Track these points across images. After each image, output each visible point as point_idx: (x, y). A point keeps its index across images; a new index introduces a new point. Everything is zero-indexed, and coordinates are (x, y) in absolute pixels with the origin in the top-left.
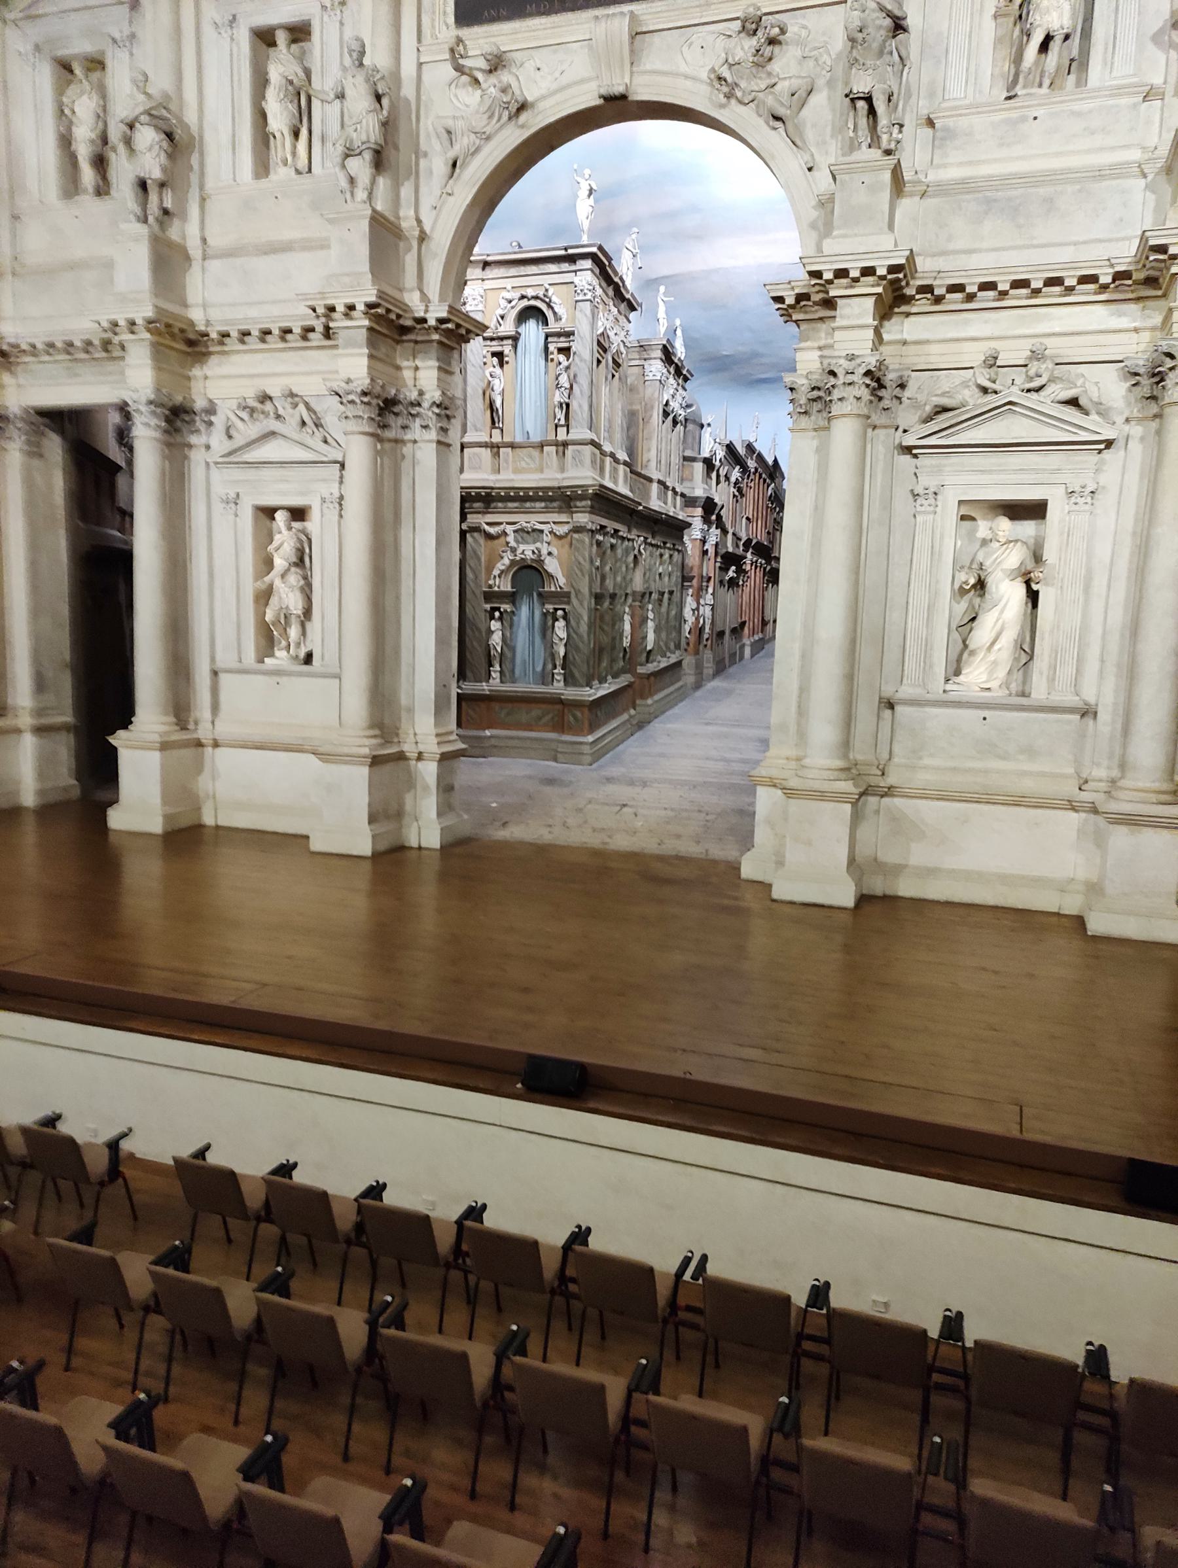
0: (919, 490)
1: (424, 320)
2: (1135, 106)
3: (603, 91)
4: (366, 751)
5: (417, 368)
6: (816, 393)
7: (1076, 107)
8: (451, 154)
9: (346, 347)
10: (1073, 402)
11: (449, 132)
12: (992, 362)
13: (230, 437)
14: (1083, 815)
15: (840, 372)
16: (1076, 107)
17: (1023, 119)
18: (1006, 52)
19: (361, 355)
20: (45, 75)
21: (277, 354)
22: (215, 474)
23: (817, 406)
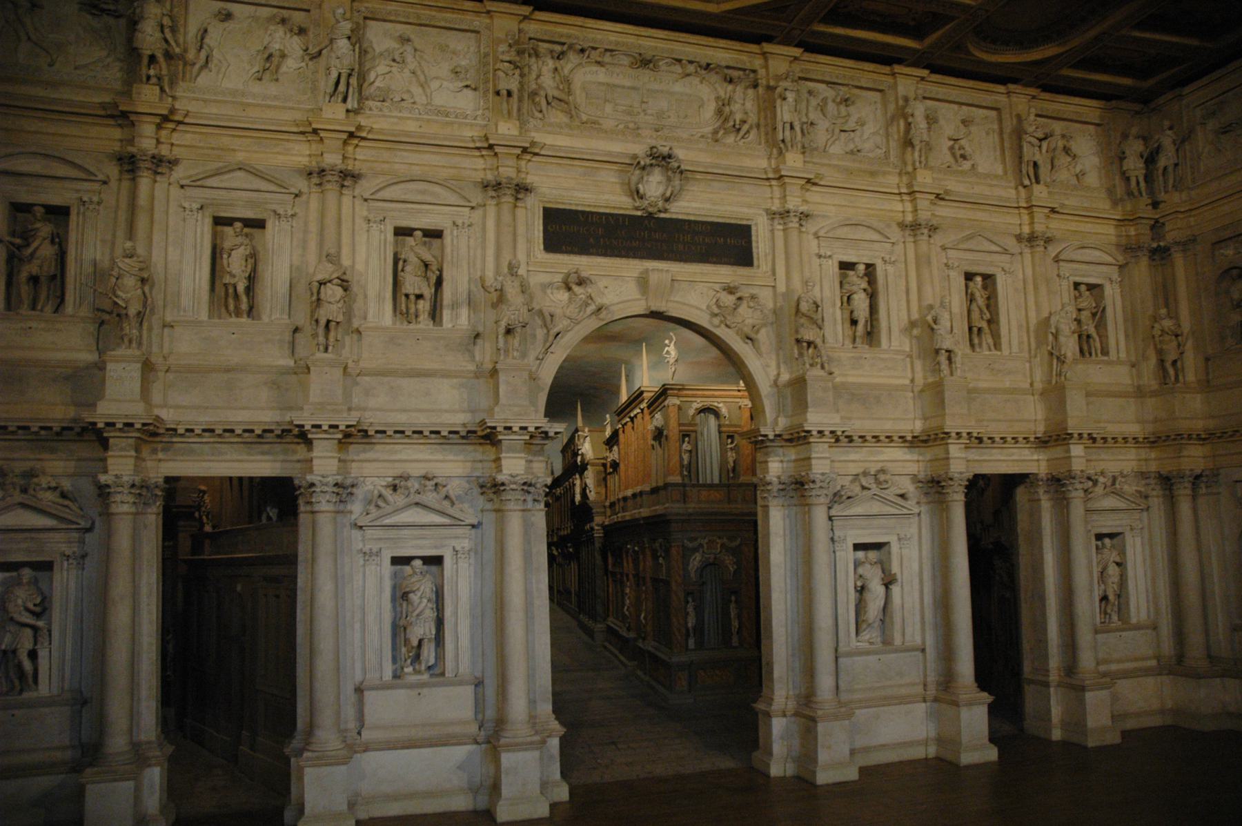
0: (836, 538)
1: (546, 433)
2: (903, 360)
3: (653, 309)
4: (537, 738)
5: (531, 461)
6: (783, 487)
7: (882, 356)
8: (555, 330)
9: (508, 452)
10: (902, 496)
11: (552, 316)
12: (865, 474)
13: (378, 506)
14: (928, 704)
15: (817, 480)
16: (882, 356)
17: (861, 358)
18: (847, 325)
19: (521, 458)
20: (205, 228)
21: (415, 446)
22: (356, 534)
23: (782, 493)
